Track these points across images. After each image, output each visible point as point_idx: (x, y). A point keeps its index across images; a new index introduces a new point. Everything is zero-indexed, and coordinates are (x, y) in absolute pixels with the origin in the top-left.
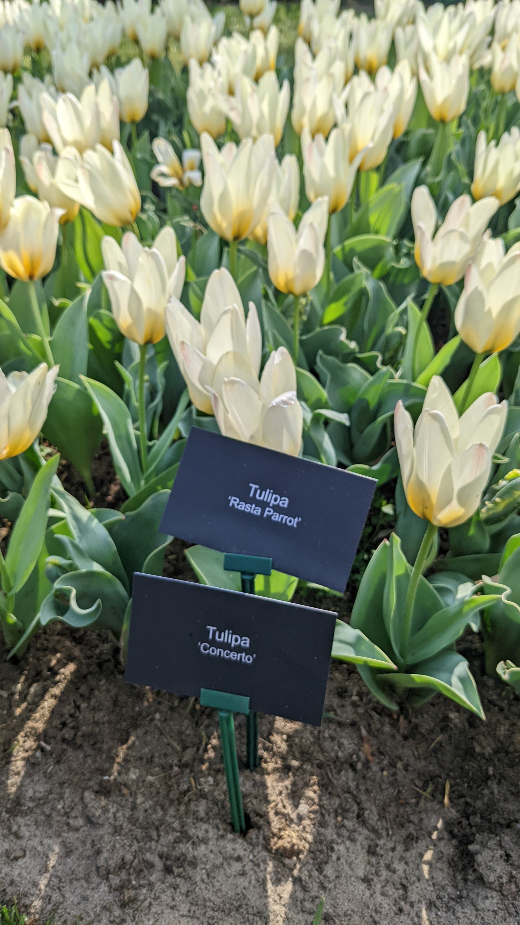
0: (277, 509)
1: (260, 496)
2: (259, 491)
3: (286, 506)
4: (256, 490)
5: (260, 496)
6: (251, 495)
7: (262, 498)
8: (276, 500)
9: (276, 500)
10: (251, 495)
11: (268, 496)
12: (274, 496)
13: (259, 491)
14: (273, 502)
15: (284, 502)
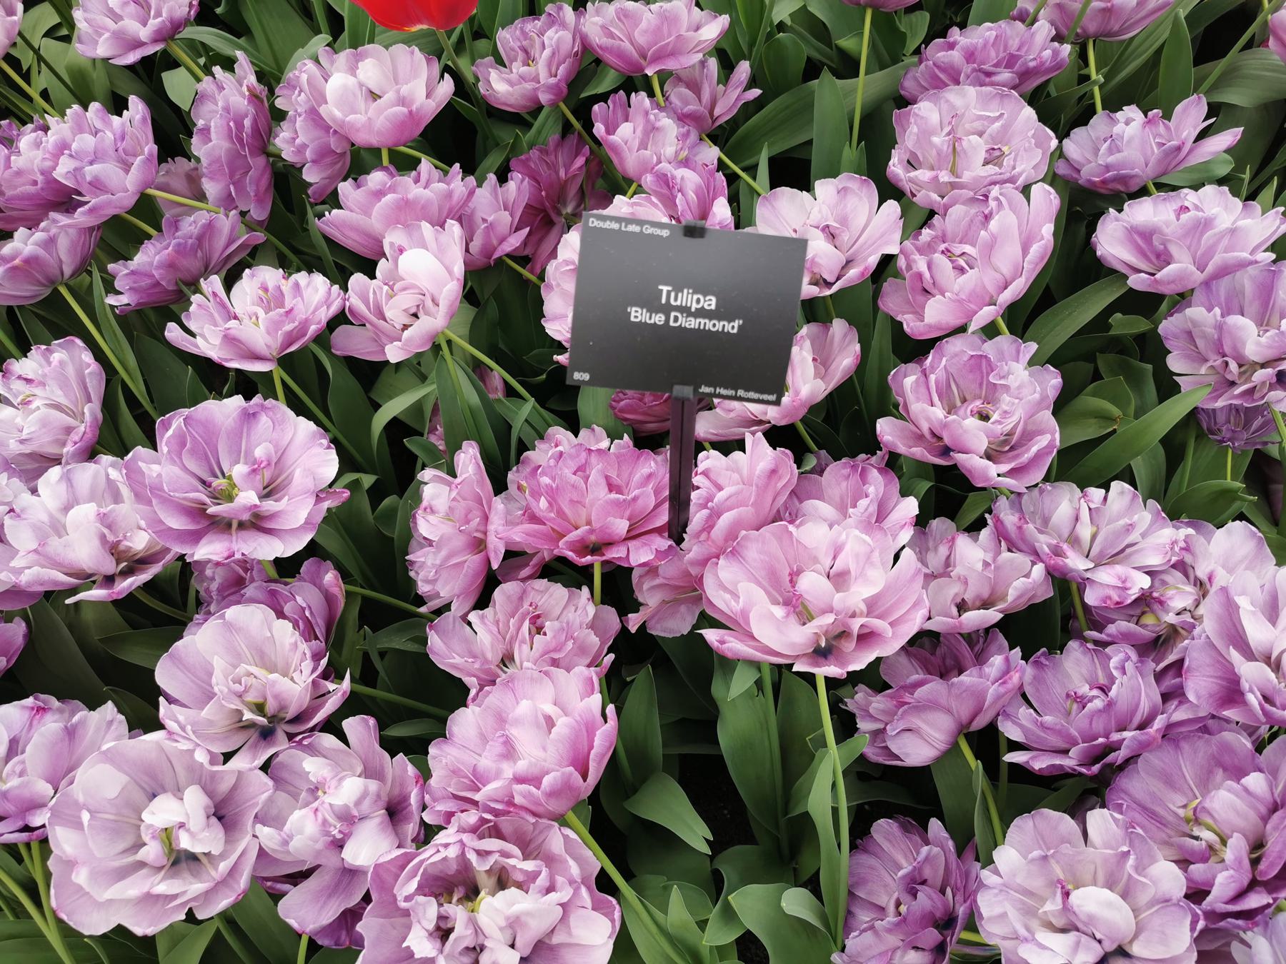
0: (701, 313)
1: (676, 299)
2: (673, 295)
3: (713, 307)
4: (669, 293)
5: (676, 299)
6: (664, 301)
7: (678, 303)
8: (698, 301)
9: (698, 301)
10: (664, 301)
11: (687, 298)
12: (695, 297)
13: (673, 295)
14: (694, 307)
15: (711, 303)
